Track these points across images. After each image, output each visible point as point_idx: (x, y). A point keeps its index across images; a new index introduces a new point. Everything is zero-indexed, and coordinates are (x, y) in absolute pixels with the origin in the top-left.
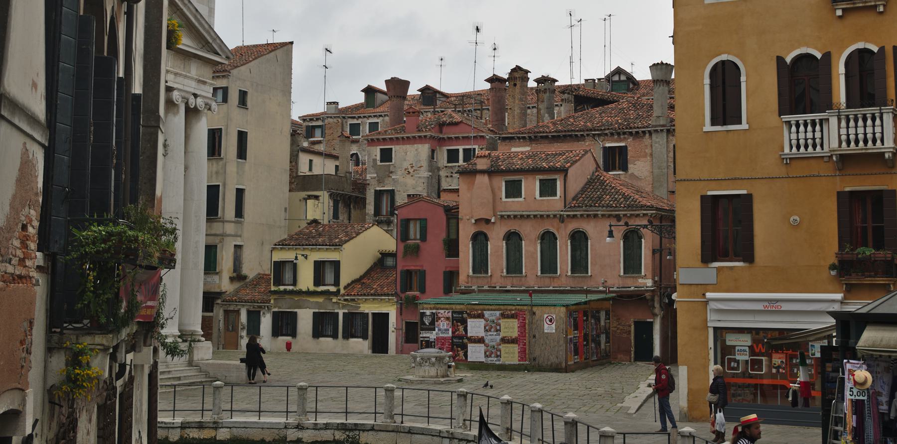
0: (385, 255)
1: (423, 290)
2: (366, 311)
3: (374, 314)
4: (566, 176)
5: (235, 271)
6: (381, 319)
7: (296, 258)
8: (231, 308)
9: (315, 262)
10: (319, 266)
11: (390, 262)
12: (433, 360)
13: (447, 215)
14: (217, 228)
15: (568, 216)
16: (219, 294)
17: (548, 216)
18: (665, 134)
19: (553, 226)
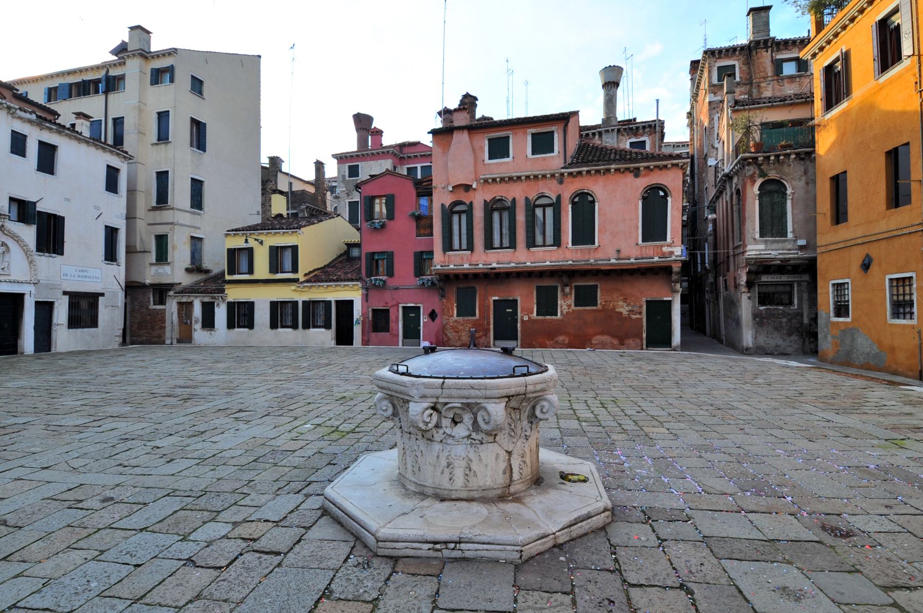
0: (350, 246)
1: (390, 273)
2: (328, 299)
3: (337, 302)
4: (566, 125)
5: (192, 263)
6: (345, 307)
7: (246, 241)
8: (184, 300)
9: (271, 247)
10: (276, 253)
11: (355, 252)
12: (497, 410)
13: (417, 189)
14: (166, 216)
15: (570, 174)
16: (170, 286)
17: (544, 176)
18: (615, 133)
19: (551, 190)
